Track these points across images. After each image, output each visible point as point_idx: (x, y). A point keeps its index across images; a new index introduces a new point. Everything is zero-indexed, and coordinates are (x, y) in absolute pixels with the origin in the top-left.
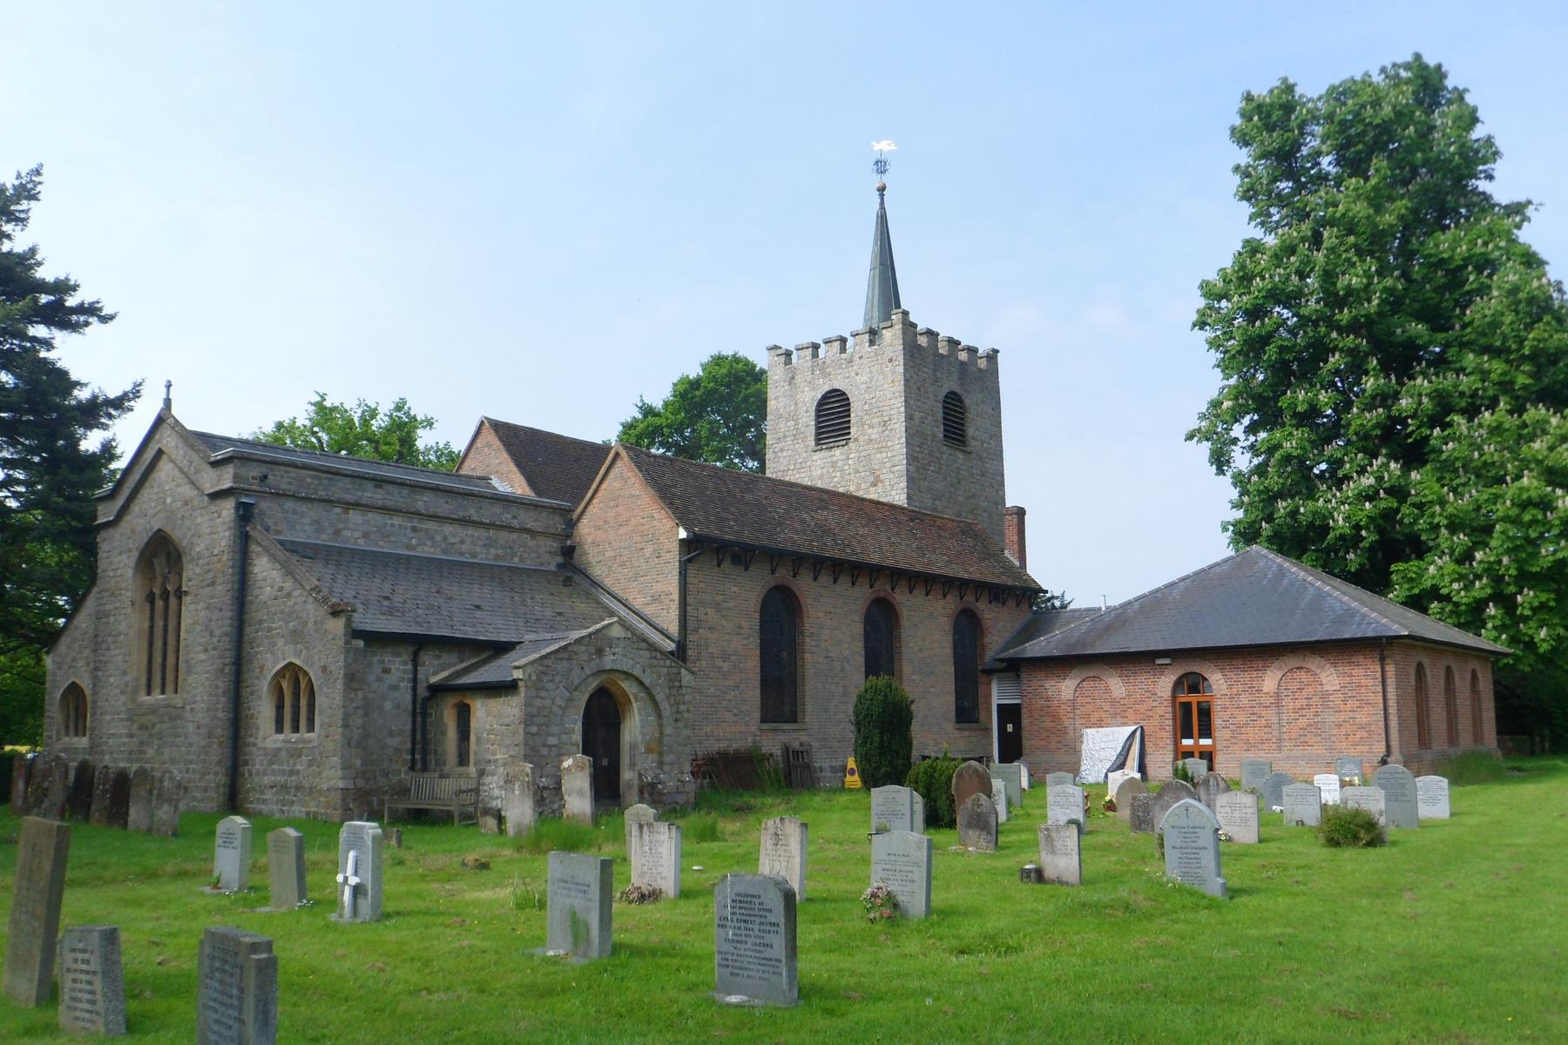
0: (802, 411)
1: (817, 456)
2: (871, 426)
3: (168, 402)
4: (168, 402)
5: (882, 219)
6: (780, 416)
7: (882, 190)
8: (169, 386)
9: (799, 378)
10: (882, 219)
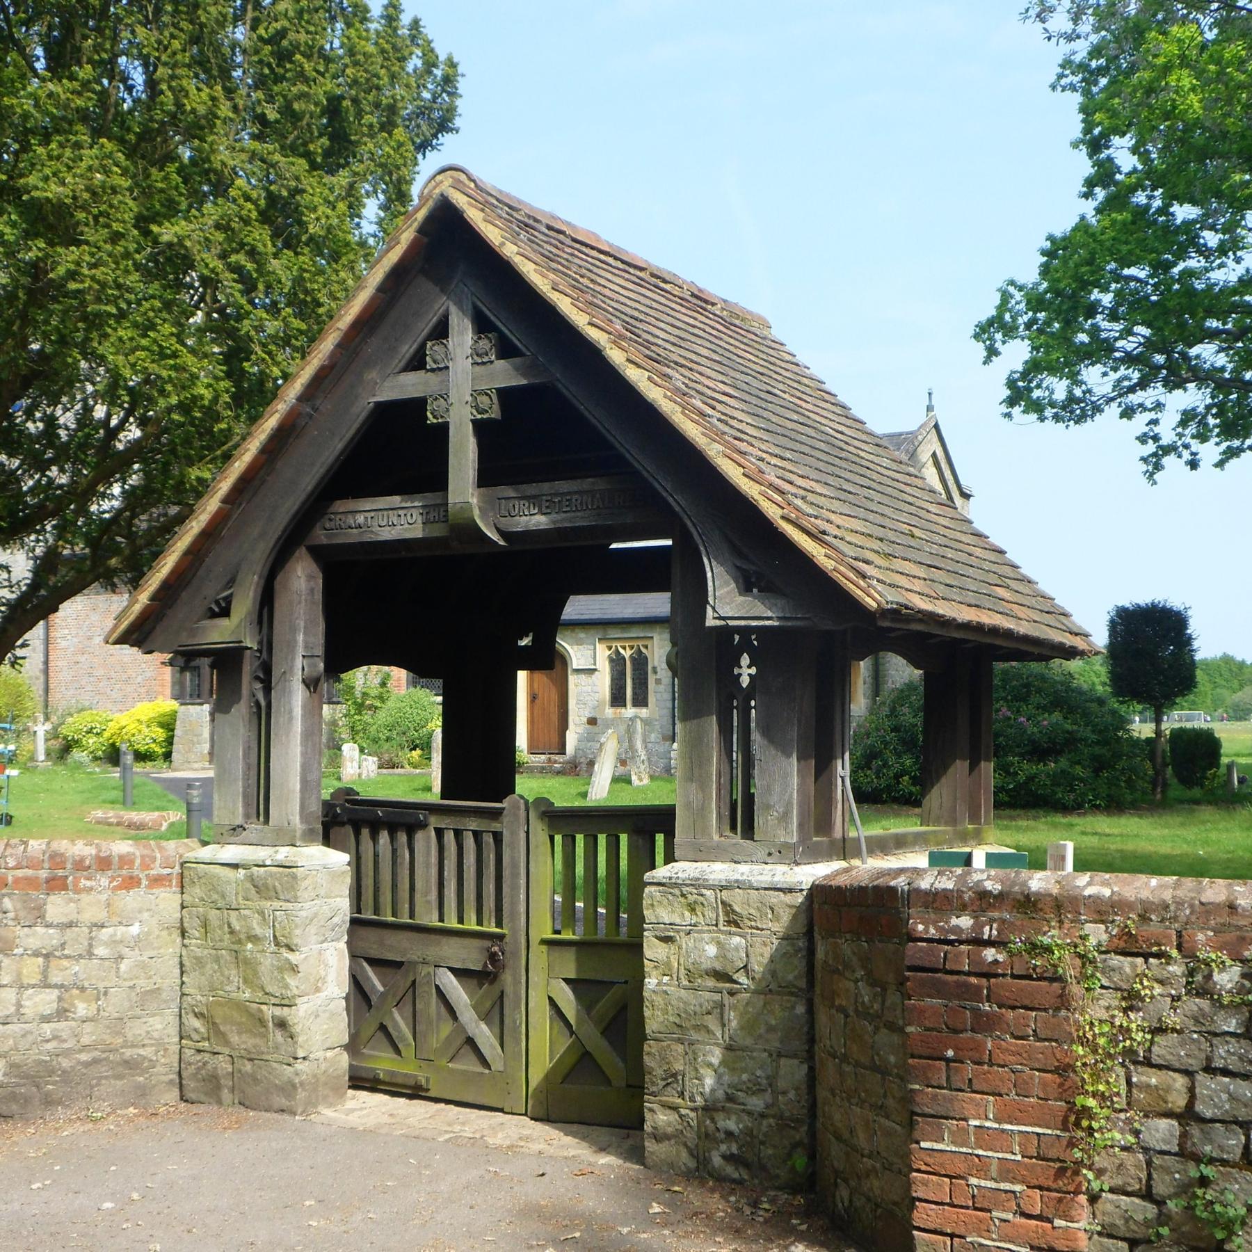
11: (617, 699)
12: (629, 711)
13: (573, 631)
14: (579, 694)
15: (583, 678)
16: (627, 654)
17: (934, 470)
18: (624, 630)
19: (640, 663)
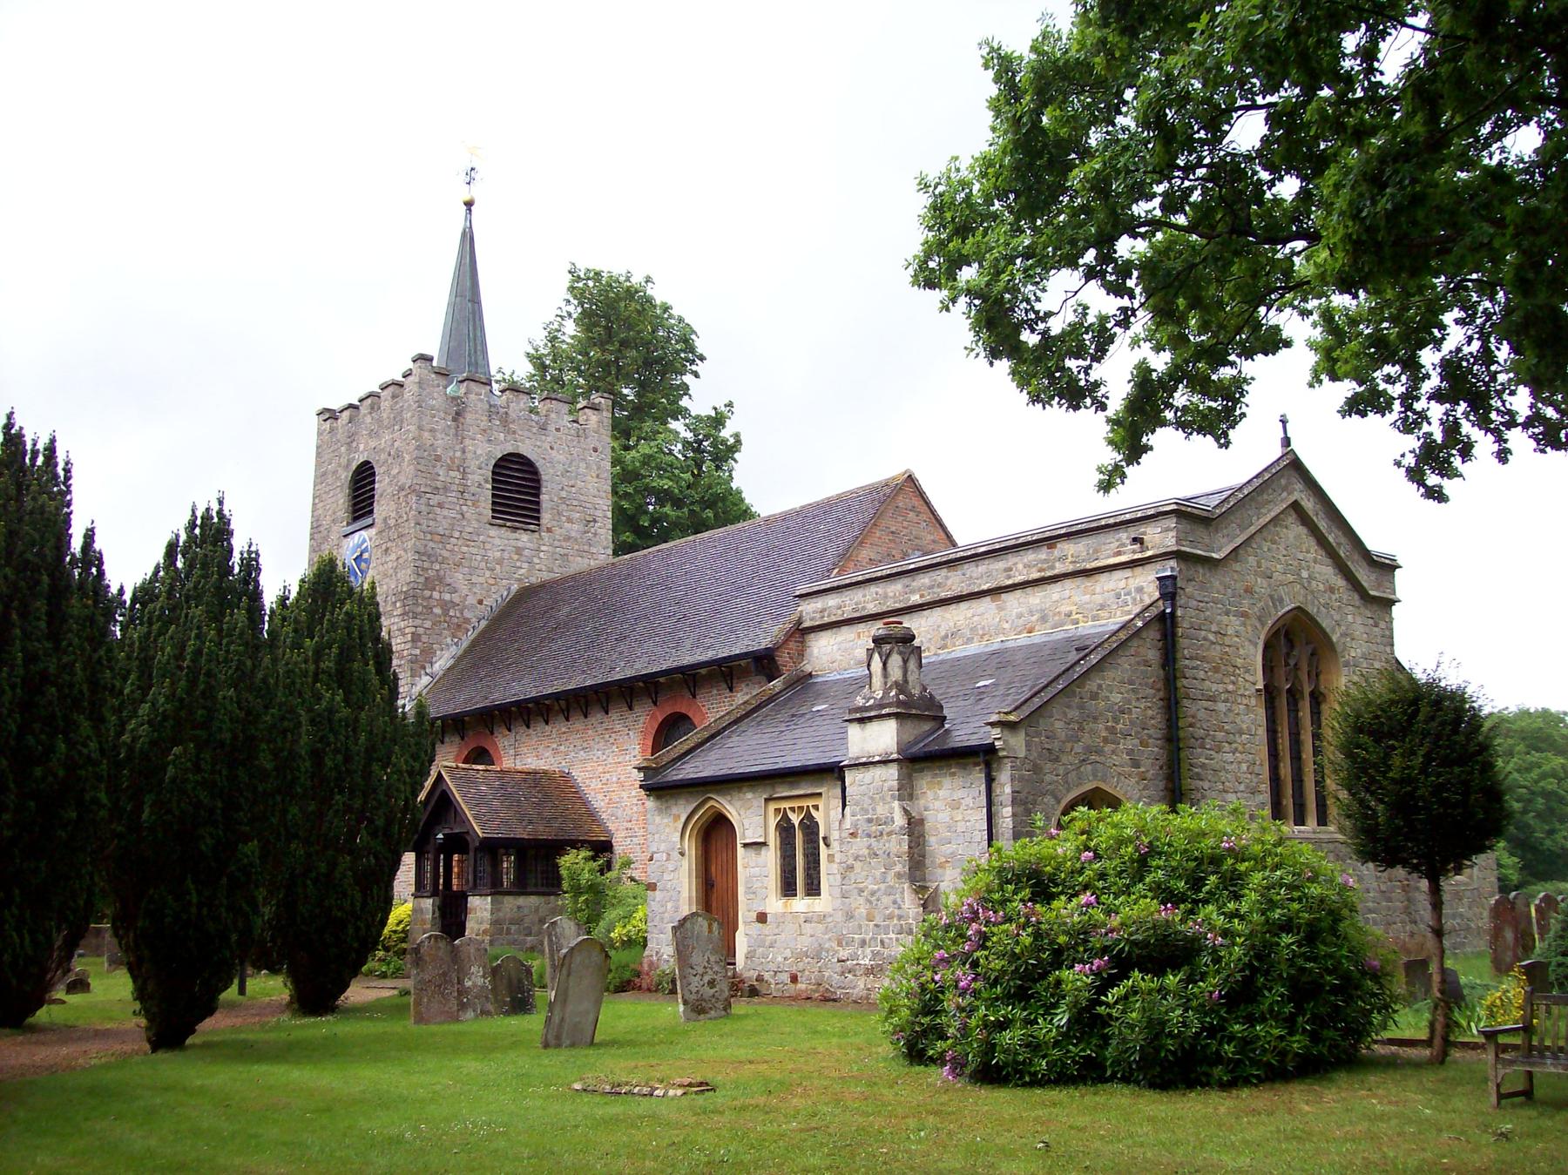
0: (473, 465)
1: (493, 532)
2: (570, 520)
3: (1286, 441)
4: (1286, 441)
5: (468, 238)
6: (438, 458)
7: (469, 204)
8: (1284, 422)
9: (469, 418)
10: (468, 238)
11: (788, 889)
12: (800, 904)
13: (740, 789)
14: (749, 879)
15: (751, 853)
16: (795, 819)
17: (1302, 530)
18: (793, 785)
19: (810, 827)
